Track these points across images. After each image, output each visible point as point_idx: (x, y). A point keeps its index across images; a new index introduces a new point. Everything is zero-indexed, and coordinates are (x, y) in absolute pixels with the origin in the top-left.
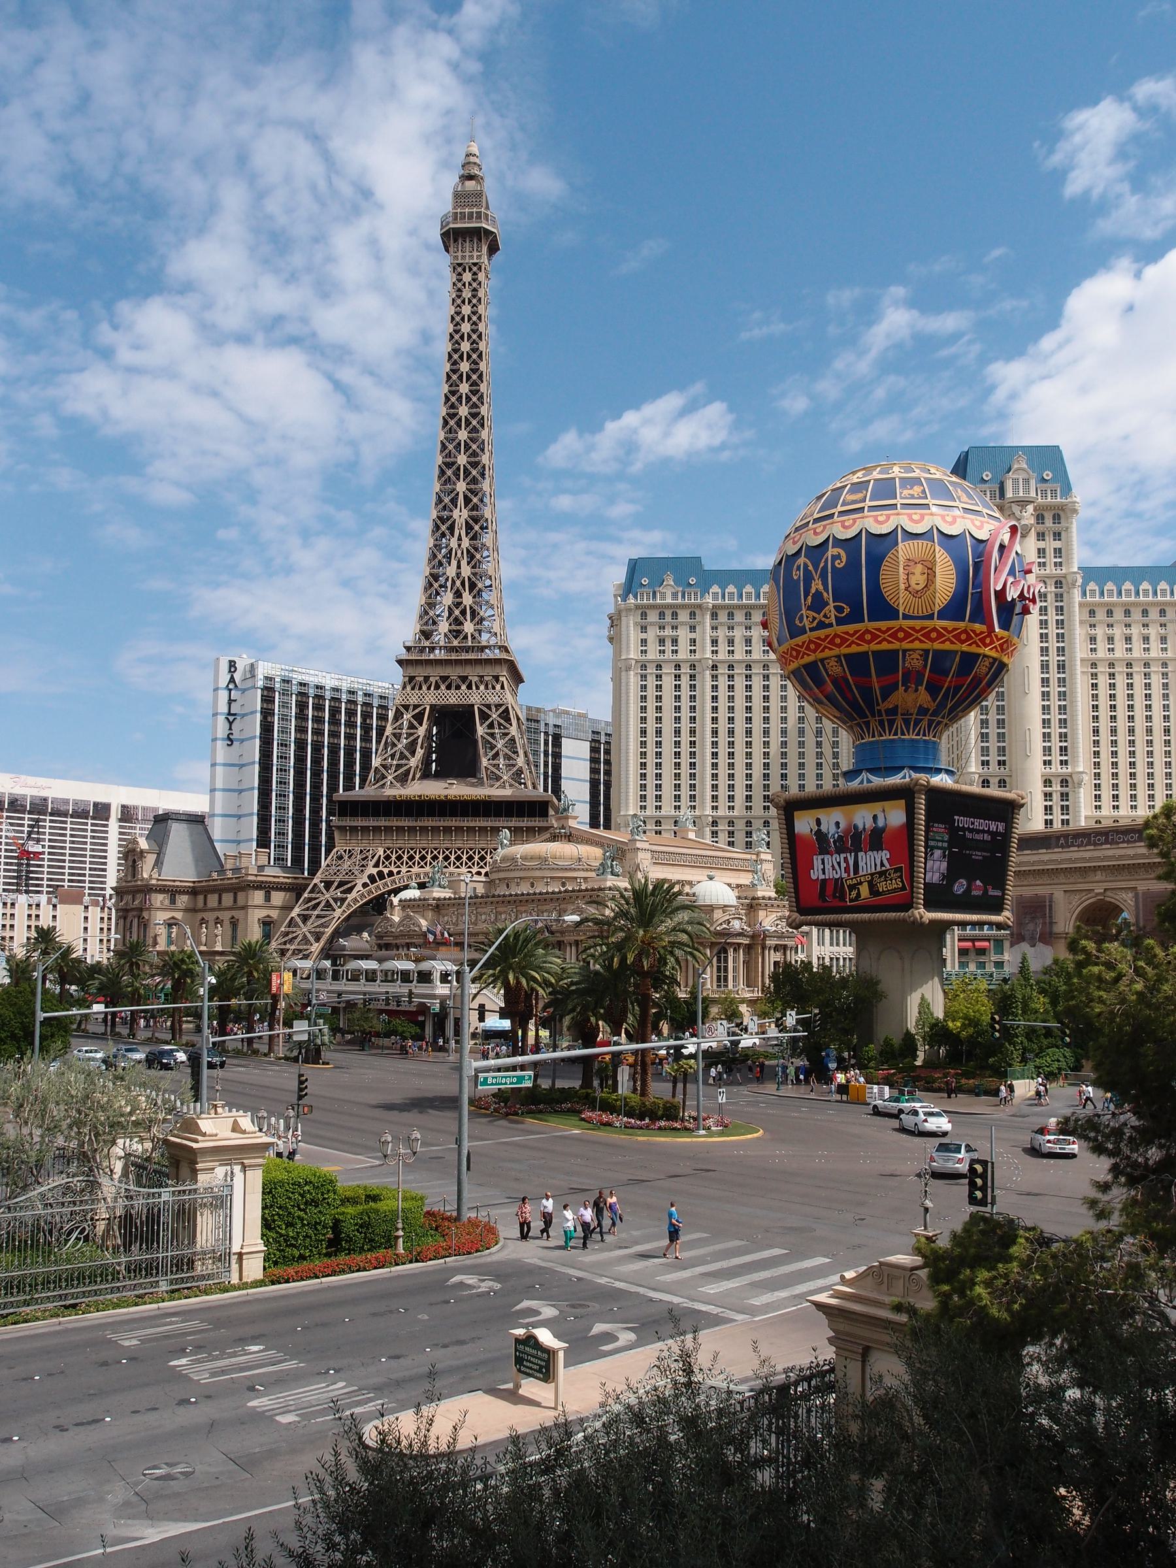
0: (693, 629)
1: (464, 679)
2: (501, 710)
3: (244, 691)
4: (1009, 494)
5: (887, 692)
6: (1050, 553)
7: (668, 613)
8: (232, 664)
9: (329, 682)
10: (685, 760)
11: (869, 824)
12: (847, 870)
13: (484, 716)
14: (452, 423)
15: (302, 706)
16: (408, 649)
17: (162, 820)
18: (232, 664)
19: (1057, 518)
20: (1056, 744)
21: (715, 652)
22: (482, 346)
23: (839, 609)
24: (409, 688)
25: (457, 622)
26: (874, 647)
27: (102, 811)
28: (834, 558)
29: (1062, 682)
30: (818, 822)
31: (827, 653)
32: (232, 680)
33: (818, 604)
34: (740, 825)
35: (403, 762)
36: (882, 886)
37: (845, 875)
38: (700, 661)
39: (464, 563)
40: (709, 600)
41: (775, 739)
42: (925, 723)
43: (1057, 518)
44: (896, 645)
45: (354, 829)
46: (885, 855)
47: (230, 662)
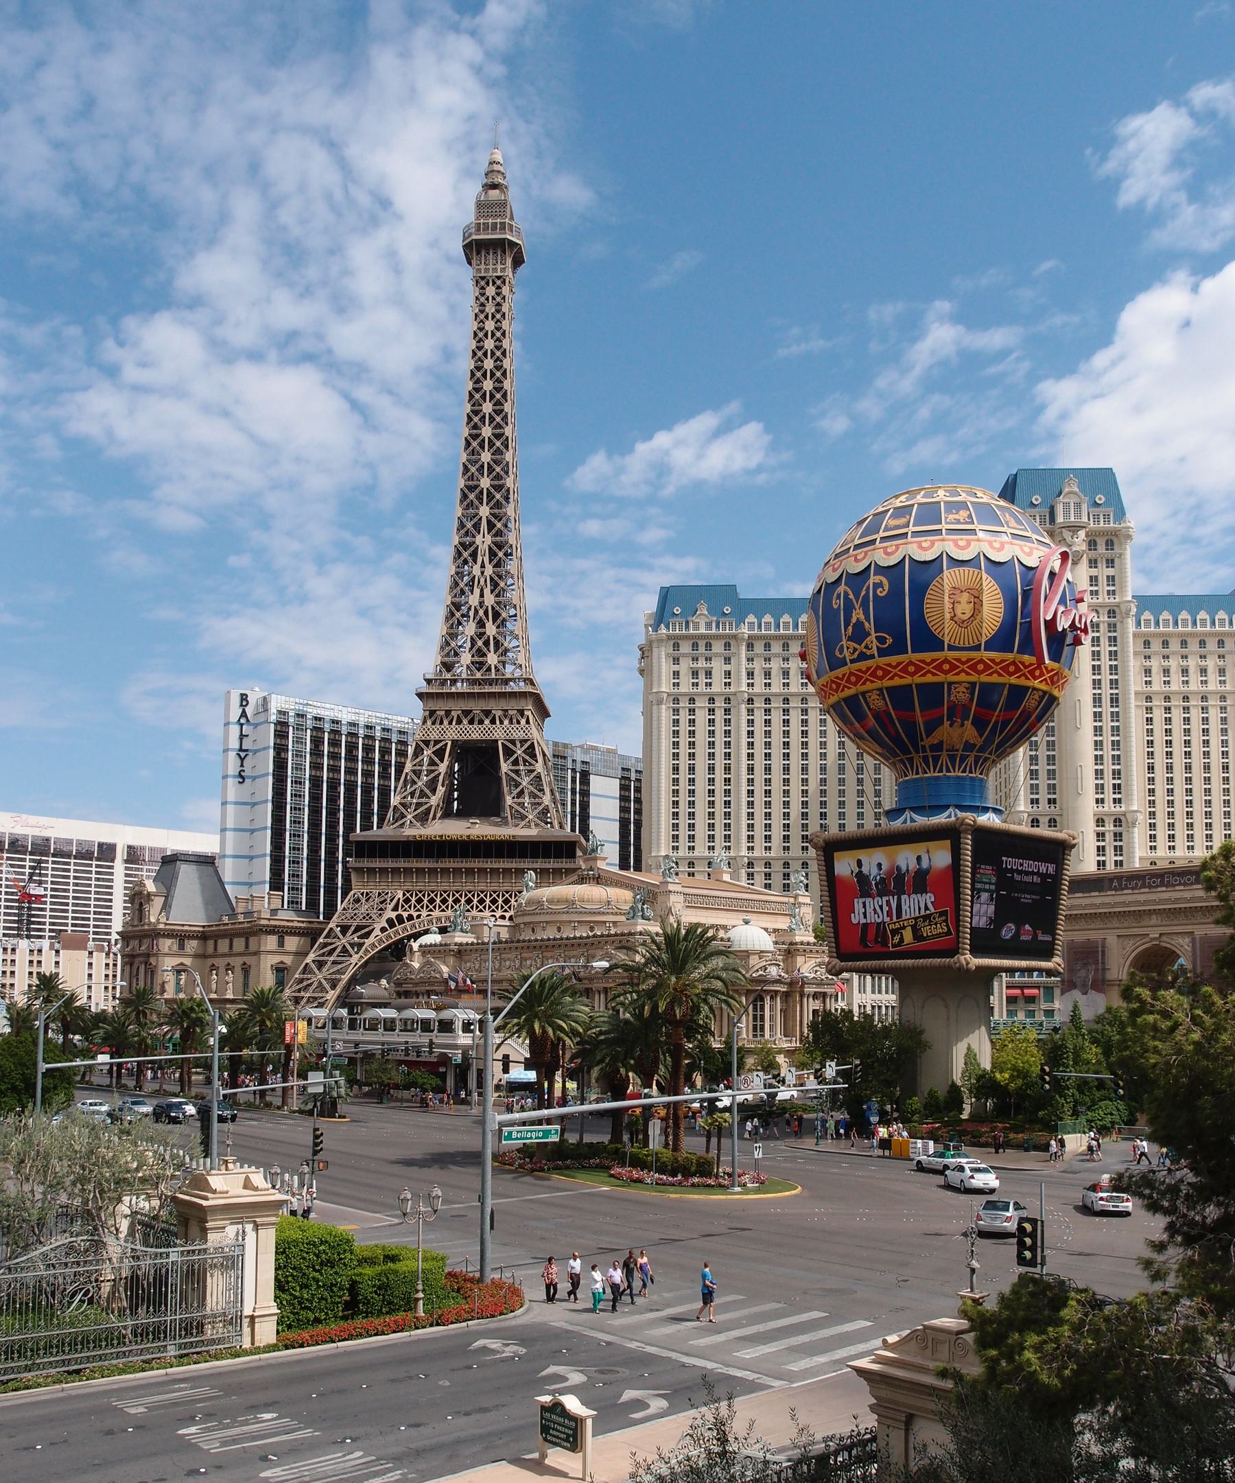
0: (727, 660)
1: (487, 713)
2: (526, 746)
3: (256, 725)
4: (1060, 519)
5: (931, 727)
6: (1103, 581)
7: (702, 644)
8: (244, 698)
9: (346, 716)
11: (913, 865)
12: (889, 914)
13: (509, 753)
14: (475, 444)
15: (317, 742)
16: (429, 681)
17: (170, 861)
18: (244, 698)
19: (1110, 544)
20: (1109, 781)
21: (750, 685)
22: (506, 363)
23: (881, 640)
24: (429, 722)
25: (480, 653)
26: (918, 679)
27: (107, 851)
28: (876, 586)
29: (1116, 716)
30: (859, 863)
31: (869, 686)
32: (244, 714)
33: (859, 634)
34: (777, 867)
35: (423, 800)
36: (926, 931)
37: (887, 919)
38: (735, 694)
39: (487, 591)
40: (745, 631)
41: (814, 776)
42: (971, 760)
43: (1110, 544)
44: (941, 678)
45: (371, 871)
46: (929, 898)
47: (242, 695)
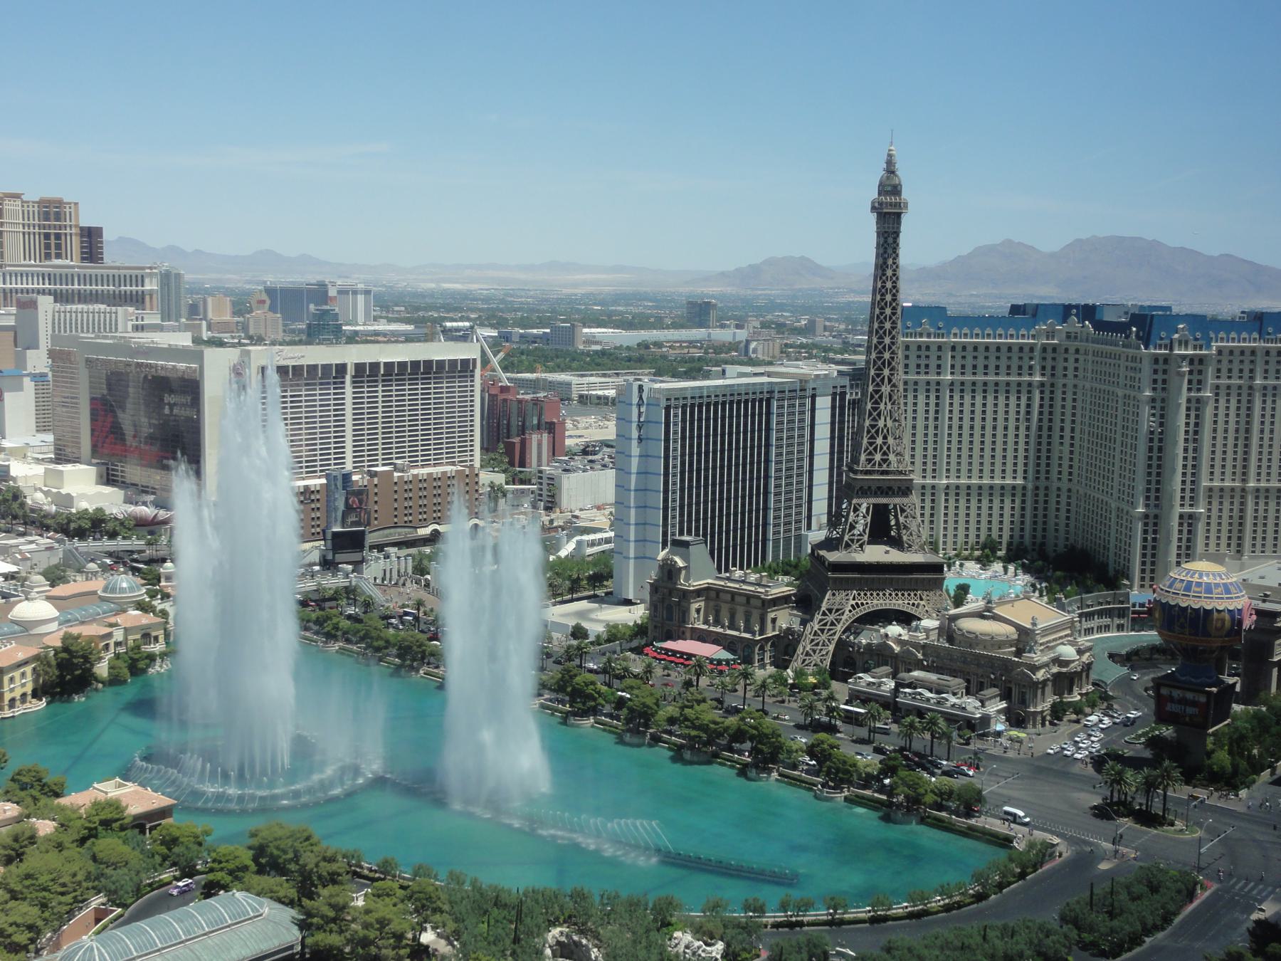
10: (930, 446)
15: (684, 413)
29: (1195, 458)
